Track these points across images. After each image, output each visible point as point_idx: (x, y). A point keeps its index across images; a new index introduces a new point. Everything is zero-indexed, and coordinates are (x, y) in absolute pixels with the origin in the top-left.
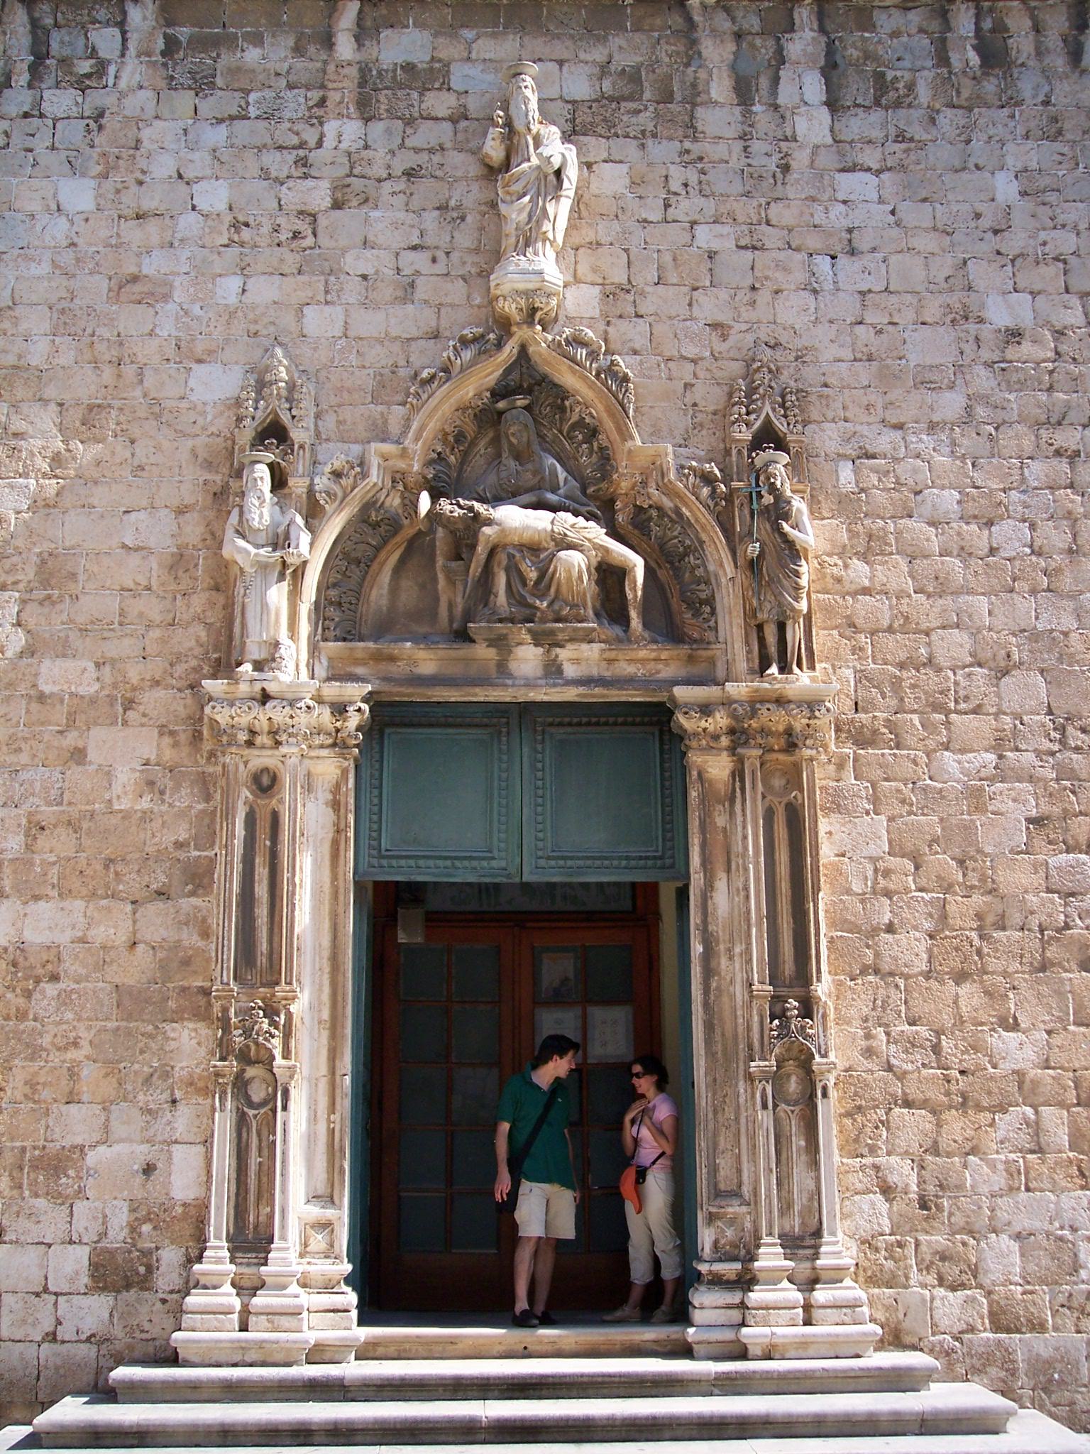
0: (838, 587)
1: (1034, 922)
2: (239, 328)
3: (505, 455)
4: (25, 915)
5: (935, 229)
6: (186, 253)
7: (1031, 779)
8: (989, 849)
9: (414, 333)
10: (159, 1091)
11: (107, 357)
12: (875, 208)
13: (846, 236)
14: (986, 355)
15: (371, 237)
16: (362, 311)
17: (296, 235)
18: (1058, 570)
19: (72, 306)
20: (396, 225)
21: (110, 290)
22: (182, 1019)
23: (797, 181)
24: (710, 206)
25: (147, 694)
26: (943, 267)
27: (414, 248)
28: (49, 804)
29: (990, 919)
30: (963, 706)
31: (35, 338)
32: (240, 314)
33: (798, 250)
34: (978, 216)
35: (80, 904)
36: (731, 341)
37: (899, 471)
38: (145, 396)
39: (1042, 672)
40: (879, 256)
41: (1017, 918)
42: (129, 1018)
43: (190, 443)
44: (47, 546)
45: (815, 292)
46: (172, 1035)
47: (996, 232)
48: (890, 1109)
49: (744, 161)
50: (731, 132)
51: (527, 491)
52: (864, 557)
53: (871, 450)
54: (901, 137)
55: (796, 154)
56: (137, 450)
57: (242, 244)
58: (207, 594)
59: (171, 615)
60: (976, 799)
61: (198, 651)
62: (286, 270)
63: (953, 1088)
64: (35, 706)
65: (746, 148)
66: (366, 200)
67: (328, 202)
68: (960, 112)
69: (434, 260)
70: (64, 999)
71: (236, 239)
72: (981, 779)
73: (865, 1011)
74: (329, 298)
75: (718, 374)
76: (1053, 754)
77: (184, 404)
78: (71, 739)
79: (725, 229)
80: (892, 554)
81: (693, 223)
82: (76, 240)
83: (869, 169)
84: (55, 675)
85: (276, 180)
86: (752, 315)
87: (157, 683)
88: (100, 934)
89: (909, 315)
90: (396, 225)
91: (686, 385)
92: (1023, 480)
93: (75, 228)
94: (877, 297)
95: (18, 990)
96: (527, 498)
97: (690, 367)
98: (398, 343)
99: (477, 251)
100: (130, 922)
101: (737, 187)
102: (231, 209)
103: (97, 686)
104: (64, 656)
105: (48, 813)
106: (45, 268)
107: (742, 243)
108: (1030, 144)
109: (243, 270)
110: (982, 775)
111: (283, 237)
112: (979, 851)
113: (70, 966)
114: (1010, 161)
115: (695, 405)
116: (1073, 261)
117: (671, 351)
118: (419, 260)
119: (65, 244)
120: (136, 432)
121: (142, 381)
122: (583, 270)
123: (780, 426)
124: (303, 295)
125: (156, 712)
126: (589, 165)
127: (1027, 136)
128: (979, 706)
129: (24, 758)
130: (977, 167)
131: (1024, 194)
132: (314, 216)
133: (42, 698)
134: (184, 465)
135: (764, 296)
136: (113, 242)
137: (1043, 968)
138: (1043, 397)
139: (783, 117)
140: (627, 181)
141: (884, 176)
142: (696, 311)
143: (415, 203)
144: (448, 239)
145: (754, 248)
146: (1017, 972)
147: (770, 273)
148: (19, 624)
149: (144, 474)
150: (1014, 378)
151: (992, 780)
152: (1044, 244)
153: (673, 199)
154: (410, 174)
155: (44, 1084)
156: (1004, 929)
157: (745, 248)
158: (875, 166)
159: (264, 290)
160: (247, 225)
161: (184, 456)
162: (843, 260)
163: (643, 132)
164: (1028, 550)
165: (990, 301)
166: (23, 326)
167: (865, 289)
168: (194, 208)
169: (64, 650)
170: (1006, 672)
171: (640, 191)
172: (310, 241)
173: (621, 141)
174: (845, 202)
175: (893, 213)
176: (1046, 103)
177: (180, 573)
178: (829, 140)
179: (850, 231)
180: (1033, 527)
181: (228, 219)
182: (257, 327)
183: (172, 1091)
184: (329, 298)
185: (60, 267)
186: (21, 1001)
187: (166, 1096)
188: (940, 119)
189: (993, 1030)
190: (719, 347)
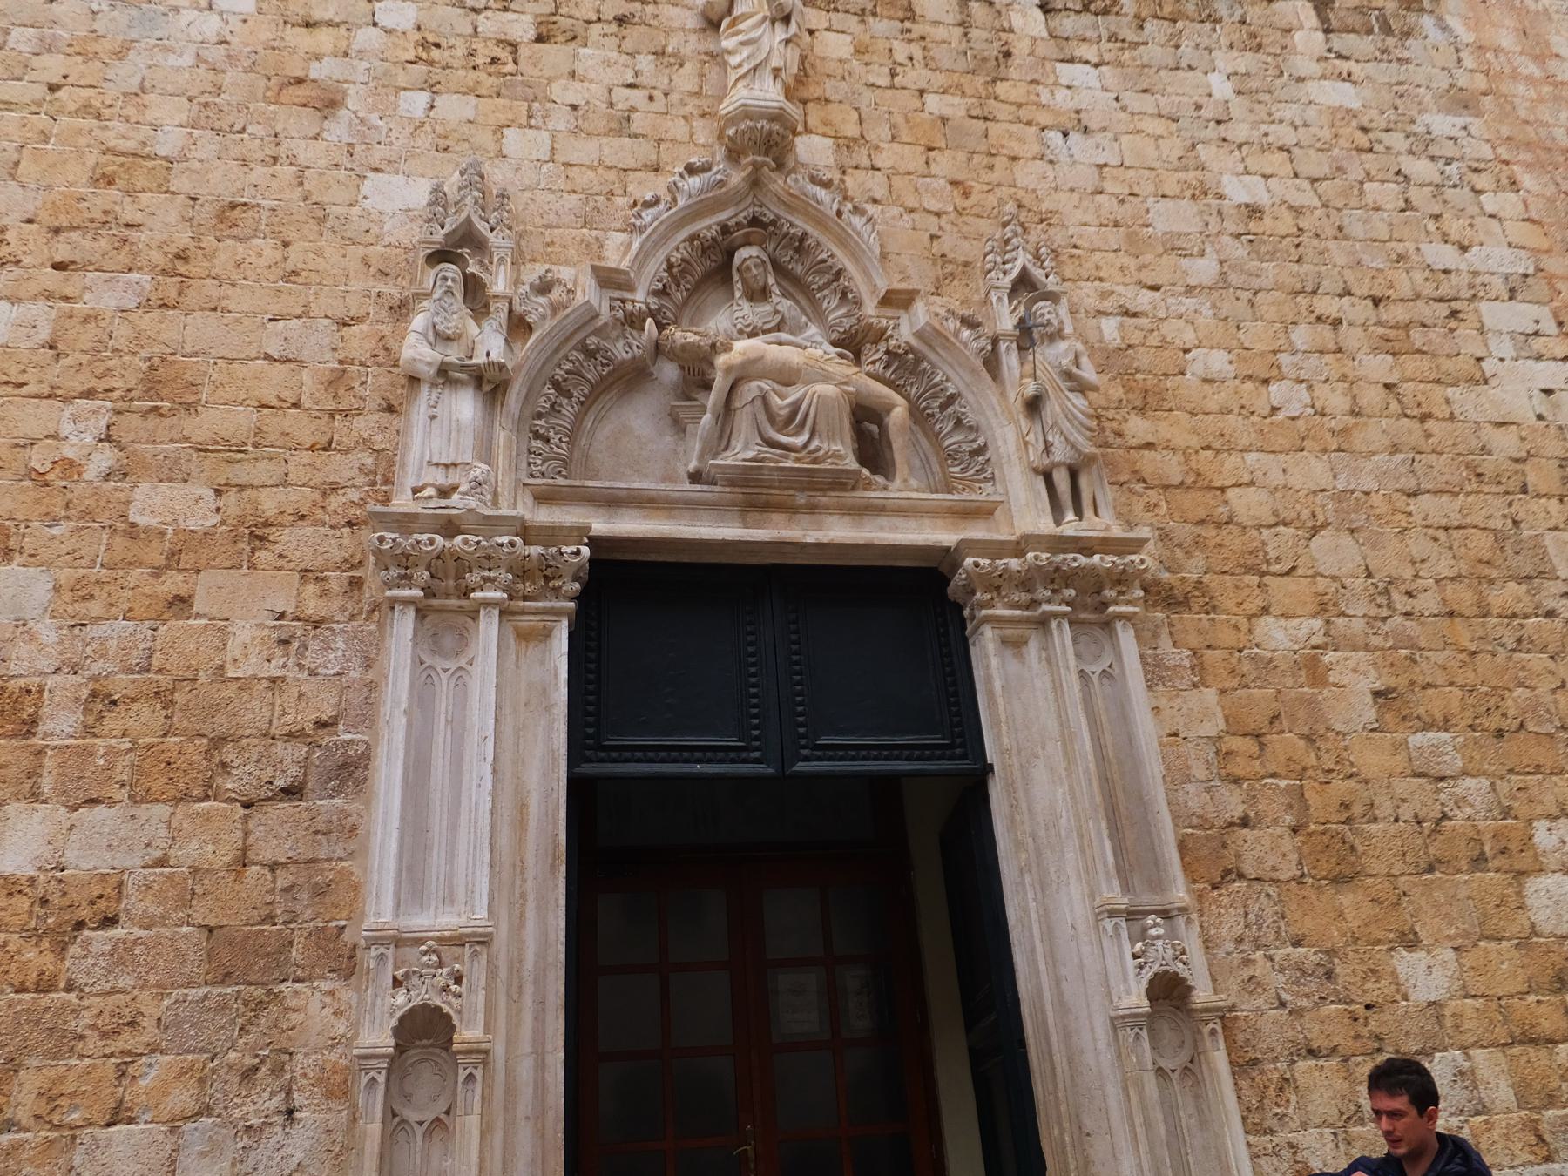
0: (1119, 441)
1: (1406, 812)
2: (424, 141)
3: (738, 294)
4: (71, 828)
5: (1160, 115)
6: (365, 64)
7: (1367, 648)
8: (1338, 727)
9: (631, 163)
10: (266, 1095)
11: (260, 155)
12: (1099, 93)
13: (1074, 116)
14: (1231, 227)
15: (580, 71)
16: (572, 138)
17: (494, 61)
18: (1345, 431)
19: (217, 100)
20: (607, 63)
21: (268, 89)
22: (311, 978)
23: (1020, 66)
24: (940, 79)
25: (287, 531)
26: (1173, 148)
27: (631, 86)
28: (127, 670)
29: (1357, 809)
30: (1275, 568)
31: (166, 128)
32: (427, 128)
33: (1029, 123)
34: (1198, 107)
35: (161, 810)
36: (974, 199)
37: (1163, 331)
38: (306, 199)
39: (1352, 531)
40: (1110, 135)
41: (1385, 808)
42: (226, 978)
43: (361, 250)
44: (158, 350)
45: (1051, 162)
46: (293, 1003)
47: (1219, 122)
48: (1294, 1062)
49: (964, 45)
50: (950, 19)
51: (765, 332)
52: (1141, 410)
53: (1133, 309)
54: (1113, 38)
55: (1015, 43)
56: (292, 256)
57: (431, 63)
58: (376, 417)
59: (327, 438)
60: (1314, 670)
61: (361, 480)
62: (483, 92)
63: (1364, 1032)
64: (119, 541)
65: (966, 34)
66: (574, 38)
67: (532, 34)
68: (1166, 23)
69: (651, 98)
70: (120, 955)
71: (424, 56)
72: (1314, 648)
73: (1238, 930)
74: (533, 122)
75: (965, 229)
76: (1384, 619)
77: (355, 211)
78: (173, 583)
79: (957, 100)
80: (1170, 410)
81: (921, 92)
82: (229, 38)
83: (1087, 62)
84: (150, 504)
85: (474, 10)
86: (994, 177)
87: (303, 517)
88: (189, 852)
89: (1150, 188)
90: (607, 63)
91: (933, 237)
92: (1291, 344)
93: (230, 27)
94: (1115, 171)
95: (45, 943)
96: (769, 337)
97: (934, 219)
98: (613, 172)
99: (698, 94)
100: (239, 834)
101: (961, 65)
102: (419, 29)
103: (217, 519)
104: (170, 480)
105: (122, 684)
106: (188, 60)
107: (974, 113)
108: (1235, 53)
109: (432, 87)
110: (1315, 641)
111: (479, 61)
112: (1328, 729)
113: (135, 903)
114: (1220, 64)
115: (943, 256)
116: (1295, 150)
117: (911, 202)
118: (637, 97)
119: (215, 40)
120: (291, 235)
121: (301, 184)
122: (812, 121)
123: (1037, 273)
124: (502, 118)
125: (298, 554)
126: (811, 32)
127: (1231, 46)
128: (1294, 568)
129: (95, 608)
130: (1190, 68)
131: (1239, 93)
132: (514, 47)
133: (132, 532)
134: (352, 275)
135: (1000, 162)
136: (276, 44)
137: (1431, 869)
138: (1296, 267)
139: (999, 12)
140: (852, 49)
141: (1104, 68)
142: (934, 169)
143: (628, 45)
144: (666, 81)
145: (986, 119)
146: (1402, 874)
147: (1005, 142)
148: (109, 439)
149: (299, 280)
150: (1264, 249)
151: (1324, 647)
152: (1266, 135)
153: (899, 69)
154: (621, 20)
155: (73, 1094)
156: (1375, 820)
157: (977, 118)
158: (1095, 60)
159: (454, 108)
160: (437, 45)
161: (354, 265)
162: (1074, 137)
163: (863, 10)
164: (1310, 411)
165: (1225, 179)
166: (150, 115)
167: (1102, 162)
168: (375, 24)
169: (173, 473)
170: (1315, 531)
171: (866, 58)
172: (510, 67)
173: (841, 15)
174: (1069, 87)
175: (1117, 99)
176: (1243, 22)
177: (341, 391)
178: (1045, 34)
179: (1078, 112)
180: (1310, 388)
181: (417, 36)
182: (448, 143)
183: (289, 1093)
184: (533, 122)
185: (206, 62)
186: (50, 957)
187: (277, 1102)
188: (1148, 25)
189: (1392, 949)
190: (960, 202)
